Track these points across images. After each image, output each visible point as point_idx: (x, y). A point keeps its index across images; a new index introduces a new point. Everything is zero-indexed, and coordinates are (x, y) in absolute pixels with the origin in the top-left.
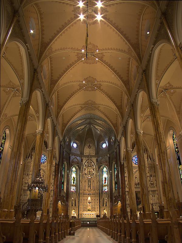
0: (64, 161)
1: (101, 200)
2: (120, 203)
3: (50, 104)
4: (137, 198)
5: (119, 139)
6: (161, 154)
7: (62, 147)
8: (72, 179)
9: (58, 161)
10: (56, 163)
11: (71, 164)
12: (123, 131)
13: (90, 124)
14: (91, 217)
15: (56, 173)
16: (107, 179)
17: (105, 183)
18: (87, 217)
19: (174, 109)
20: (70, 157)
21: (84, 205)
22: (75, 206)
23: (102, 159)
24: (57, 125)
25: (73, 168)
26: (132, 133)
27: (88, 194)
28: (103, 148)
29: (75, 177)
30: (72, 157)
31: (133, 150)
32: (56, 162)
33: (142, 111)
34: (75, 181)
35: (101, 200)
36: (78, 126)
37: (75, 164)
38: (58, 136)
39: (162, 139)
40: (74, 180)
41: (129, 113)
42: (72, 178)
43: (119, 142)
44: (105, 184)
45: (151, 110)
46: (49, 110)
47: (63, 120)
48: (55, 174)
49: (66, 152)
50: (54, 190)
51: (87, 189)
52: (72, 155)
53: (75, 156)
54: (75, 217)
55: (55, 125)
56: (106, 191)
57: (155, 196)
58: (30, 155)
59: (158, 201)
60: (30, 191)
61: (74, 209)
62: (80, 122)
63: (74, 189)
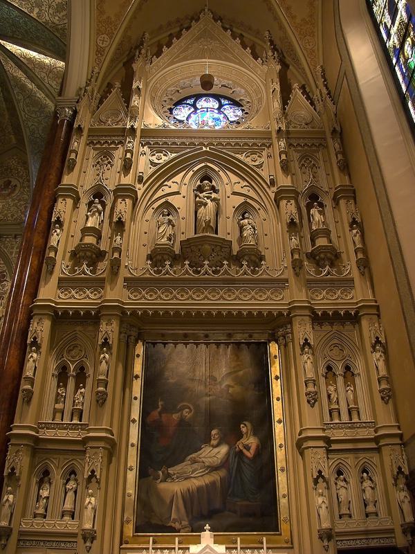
57: (359, 366)
59: (385, 418)
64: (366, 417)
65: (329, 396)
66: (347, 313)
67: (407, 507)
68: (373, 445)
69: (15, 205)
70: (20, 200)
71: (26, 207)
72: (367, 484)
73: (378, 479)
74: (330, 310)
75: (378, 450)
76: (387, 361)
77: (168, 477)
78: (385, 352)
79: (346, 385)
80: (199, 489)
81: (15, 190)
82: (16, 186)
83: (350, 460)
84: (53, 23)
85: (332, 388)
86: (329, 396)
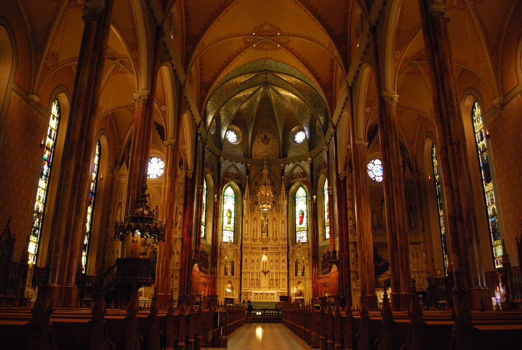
0: (207, 173)
1: (292, 264)
2: (334, 268)
3: (166, 27)
4: (377, 258)
5: (334, 120)
6: (449, 147)
7: (201, 138)
8: (225, 215)
9: (192, 172)
10: (186, 176)
11: (223, 180)
12: (347, 99)
13: (266, 84)
14: (269, 301)
15: (188, 200)
16: (305, 215)
17: (301, 223)
18: (259, 301)
19: (483, 40)
20: (219, 165)
21: (253, 273)
22: (233, 274)
23: (294, 168)
24: (187, 85)
25: (226, 188)
26: (368, 104)
27: (263, 249)
28: (296, 142)
29: (232, 209)
30: (225, 164)
31: (369, 145)
32: (186, 173)
33: (399, 46)
34: (232, 220)
35: (292, 264)
36: (237, 90)
38: (191, 112)
39: (453, 107)
40: (230, 217)
41: (365, 53)
42: (226, 212)
43: (335, 128)
44: (301, 226)
45: (427, 34)
46: (165, 45)
47: (202, 74)
48: (185, 201)
49: (210, 151)
50: (182, 239)
51: (259, 236)
52: (225, 159)
53: (231, 161)
54: (232, 300)
55: (182, 83)
56: (304, 241)
58: (123, 158)
59: (425, 266)
60: (122, 239)
61: (230, 282)
62: (242, 79)
63: (229, 237)
64: (420, 265)
65: (413, 261)
66: (418, 243)
67: (427, 285)
68: (421, 272)
69: (271, 148)
70: (273, 146)
71: (276, 149)
72: (420, 279)
73: (422, 279)
74: (414, 241)
75: (423, 273)
76: (426, 255)
77: (380, 277)
78: (426, 252)
79: (417, 258)
80: (386, 279)
81: (269, 140)
82: (269, 138)
83: (417, 275)
84: (301, 89)
85: (413, 259)
86: (413, 261)
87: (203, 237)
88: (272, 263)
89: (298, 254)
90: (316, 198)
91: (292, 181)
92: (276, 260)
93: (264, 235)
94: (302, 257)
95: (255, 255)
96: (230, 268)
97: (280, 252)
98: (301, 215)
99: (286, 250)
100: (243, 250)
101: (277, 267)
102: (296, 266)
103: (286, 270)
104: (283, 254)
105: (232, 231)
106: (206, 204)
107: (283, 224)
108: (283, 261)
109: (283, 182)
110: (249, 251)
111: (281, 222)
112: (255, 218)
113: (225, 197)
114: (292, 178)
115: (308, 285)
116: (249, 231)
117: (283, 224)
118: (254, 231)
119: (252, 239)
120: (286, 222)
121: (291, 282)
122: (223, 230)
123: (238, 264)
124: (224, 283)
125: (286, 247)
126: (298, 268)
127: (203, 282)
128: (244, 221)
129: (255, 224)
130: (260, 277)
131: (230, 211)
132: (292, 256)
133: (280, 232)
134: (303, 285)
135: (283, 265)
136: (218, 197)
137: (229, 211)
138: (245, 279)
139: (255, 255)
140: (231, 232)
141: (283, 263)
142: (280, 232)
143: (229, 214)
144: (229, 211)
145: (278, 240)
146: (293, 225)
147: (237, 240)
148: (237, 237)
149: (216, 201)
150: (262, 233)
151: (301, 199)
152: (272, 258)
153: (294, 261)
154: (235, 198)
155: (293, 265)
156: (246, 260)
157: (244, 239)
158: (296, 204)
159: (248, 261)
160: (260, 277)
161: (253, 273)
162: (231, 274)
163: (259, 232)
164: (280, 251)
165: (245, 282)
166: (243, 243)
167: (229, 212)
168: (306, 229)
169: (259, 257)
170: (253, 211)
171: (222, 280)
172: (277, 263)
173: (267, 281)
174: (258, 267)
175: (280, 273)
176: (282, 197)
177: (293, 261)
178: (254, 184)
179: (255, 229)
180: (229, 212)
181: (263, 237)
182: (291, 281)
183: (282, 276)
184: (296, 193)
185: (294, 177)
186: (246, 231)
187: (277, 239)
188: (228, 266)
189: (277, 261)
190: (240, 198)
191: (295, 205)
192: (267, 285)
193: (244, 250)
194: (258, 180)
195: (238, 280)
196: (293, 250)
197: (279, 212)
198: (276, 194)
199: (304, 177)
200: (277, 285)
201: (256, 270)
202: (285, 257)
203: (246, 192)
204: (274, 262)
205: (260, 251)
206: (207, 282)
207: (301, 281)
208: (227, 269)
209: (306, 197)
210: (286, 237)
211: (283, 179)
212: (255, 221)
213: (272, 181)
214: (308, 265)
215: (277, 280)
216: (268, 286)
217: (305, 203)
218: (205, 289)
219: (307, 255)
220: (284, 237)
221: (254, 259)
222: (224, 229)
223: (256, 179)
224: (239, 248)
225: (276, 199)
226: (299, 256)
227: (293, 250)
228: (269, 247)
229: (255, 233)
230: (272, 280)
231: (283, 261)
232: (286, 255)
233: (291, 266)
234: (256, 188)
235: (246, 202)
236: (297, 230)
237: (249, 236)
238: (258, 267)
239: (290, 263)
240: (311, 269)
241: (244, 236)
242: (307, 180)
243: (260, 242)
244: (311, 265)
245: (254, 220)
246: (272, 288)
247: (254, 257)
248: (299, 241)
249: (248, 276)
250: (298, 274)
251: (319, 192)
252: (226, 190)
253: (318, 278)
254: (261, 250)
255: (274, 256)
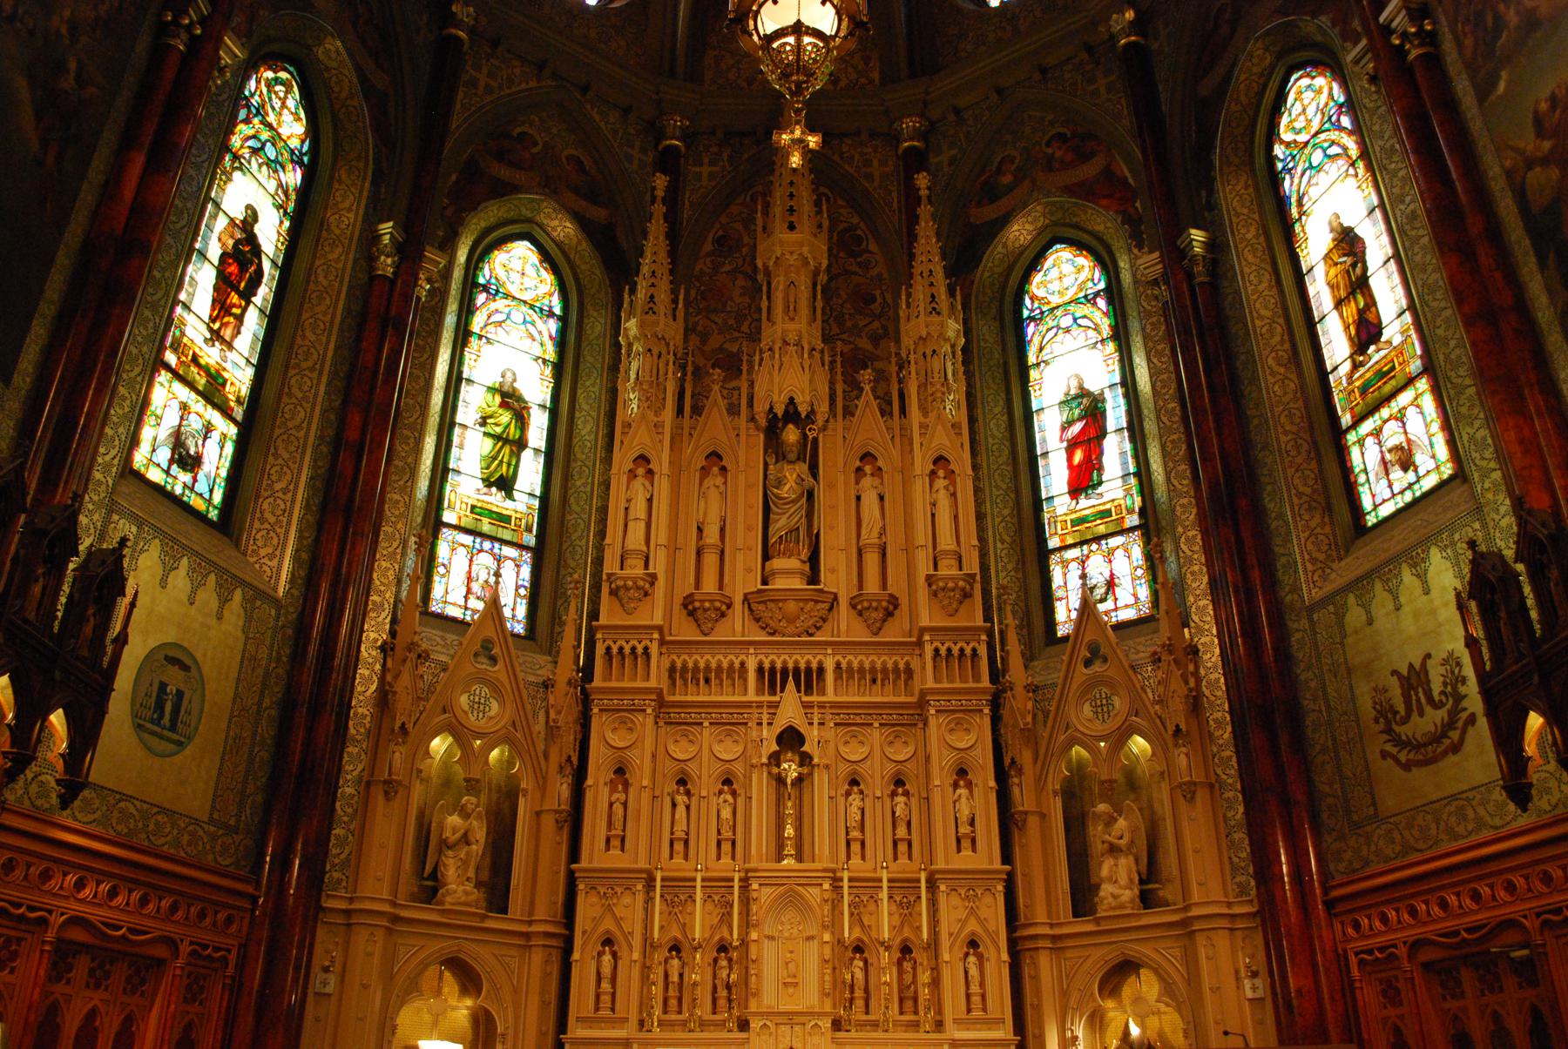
8: (467, 413)
16: (1116, 414)
17: (1083, 480)
20: (447, 59)
21: (678, 889)
22: (496, 892)
29: (536, 388)
34: (530, 473)
37: (551, 187)
42: (473, 402)
44: (1085, 504)
71: (867, 60)
87: (213, 514)
88: (855, 800)
89: (1084, 715)
90: (1210, 246)
91: (991, 212)
92: (890, 768)
93: (788, 573)
94: (1120, 738)
95: (707, 733)
96: (466, 839)
97: (923, 693)
98: (1077, 427)
99: (977, 677)
100: (597, 682)
101: (902, 832)
102: (1076, 825)
103: (987, 856)
104: (959, 716)
105: (521, 547)
106: (286, 269)
107: (941, 483)
108: (962, 772)
109: (925, 211)
110: (653, 683)
111: (922, 464)
112: (715, 456)
113: (481, 298)
114: (991, 193)
115: (1230, 983)
116: (661, 534)
117: (941, 483)
118: (699, 553)
119: (688, 602)
120: (962, 462)
121: (1045, 968)
122: (434, 524)
123: (551, 803)
124: (389, 977)
125: (983, 651)
126: (1097, 835)
127: (76, 921)
128: (622, 459)
129: (713, 495)
130: (747, 924)
131: (510, 398)
132: (1030, 737)
133: (922, 536)
134: (1168, 990)
135: (965, 812)
136: (409, 252)
137: (504, 395)
138: (608, 942)
139: (707, 733)
140: (508, 551)
141: (963, 791)
142: (922, 536)
143: (505, 417)
144: (504, 395)
145: (903, 613)
146: (1018, 503)
147: (556, 620)
148: (559, 594)
149: (386, 265)
150: (766, 557)
151: (1066, 321)
152: (855, 752)
153: (1054, 783)
154: (564, 319)
155: (1043, 816)
156: (620, 771)
157: (614, 593)
158: (1032, 359)
159: (641, 776)
160: (747, 924)
161: (678, 889)
162: (476, 895)
163: (740, 556)
164: (930, 684)
165: (606, 970)
166: (603, 620)
167: (504, 405)
168: (1134, 520)
169: (740, 749)
170: (697, 410)
171: (368, 946)
172: (900, 799)
173: (811, 961)
174: (727, 834)
175: (932, 885)
176: (920, 292)
177: (1040, 781)
178: (708, 247)
179: (712, 535)
180: (504, 405)
181: (779, 583)
182: (1044, 960)
183: (952, 909)
184: (1021, 291)
185: (1007, 179)
186: (637, 532)
187: (894, 602)
188: (454, 820)
189: (899, 782)
190: (597, 325)
191: (1024, 370)
192: (809, 996)
193: (608, 676)
194: (739, 226)
195: (537, 957)
196: (1033, 689)
197: (903, 411)
198: (876, 307)
199: (1084, 157)
200: (908, 999)
201: (704, 863)
202: (975, 740)
203: (645, 270)
204: (877, 783)
205: (752, 696)
206: (172, 944)
207: (1145, 951)
208: (444, 845)
209: (1113, 293)
210: (976, 569)
211: (924, 193)
212: (715, 480)
213: (845, 230)
214: (1202, 796)
215: (906, 950)
216: (828, 1008)
217: (1106, 332)
218: (129, 1021)
219: (1178, 706)
220: (954, 572)
221: (692, 768)
222: (448, 517)
223: (723, 219)
224: (566, 671)
225: (875, 339)
226: (1099, 727)
227: (1033, 689)
228: (829, 665)
229: (710, 560)
230: (858, 949)
231: (962, 772)
232: (987, 721)
233: (1033, 821)
234: (727, 268)
235: (642, 325)
236: (1053, 543)
237: (659, 565)
238: (727, 834)
239: (1024, 798)
240: (1240, 836)
241: (610, 566)
242: (1108, 173)
243: (754, 626)
244: (1234, 794)
245: (705, 472)
246: (861, 1025)
247: (693, 749)
248: (1087, 608)
249: (630, 907)
250: (1106, 890)
251: (1234, 196)
252: (499, 258)
253: (1329, 904)
254: (760, 691)
255: (876, 735)
